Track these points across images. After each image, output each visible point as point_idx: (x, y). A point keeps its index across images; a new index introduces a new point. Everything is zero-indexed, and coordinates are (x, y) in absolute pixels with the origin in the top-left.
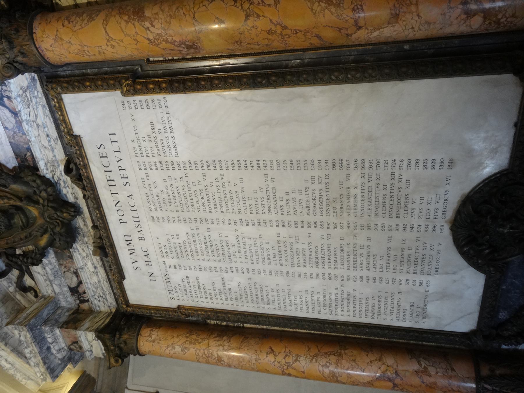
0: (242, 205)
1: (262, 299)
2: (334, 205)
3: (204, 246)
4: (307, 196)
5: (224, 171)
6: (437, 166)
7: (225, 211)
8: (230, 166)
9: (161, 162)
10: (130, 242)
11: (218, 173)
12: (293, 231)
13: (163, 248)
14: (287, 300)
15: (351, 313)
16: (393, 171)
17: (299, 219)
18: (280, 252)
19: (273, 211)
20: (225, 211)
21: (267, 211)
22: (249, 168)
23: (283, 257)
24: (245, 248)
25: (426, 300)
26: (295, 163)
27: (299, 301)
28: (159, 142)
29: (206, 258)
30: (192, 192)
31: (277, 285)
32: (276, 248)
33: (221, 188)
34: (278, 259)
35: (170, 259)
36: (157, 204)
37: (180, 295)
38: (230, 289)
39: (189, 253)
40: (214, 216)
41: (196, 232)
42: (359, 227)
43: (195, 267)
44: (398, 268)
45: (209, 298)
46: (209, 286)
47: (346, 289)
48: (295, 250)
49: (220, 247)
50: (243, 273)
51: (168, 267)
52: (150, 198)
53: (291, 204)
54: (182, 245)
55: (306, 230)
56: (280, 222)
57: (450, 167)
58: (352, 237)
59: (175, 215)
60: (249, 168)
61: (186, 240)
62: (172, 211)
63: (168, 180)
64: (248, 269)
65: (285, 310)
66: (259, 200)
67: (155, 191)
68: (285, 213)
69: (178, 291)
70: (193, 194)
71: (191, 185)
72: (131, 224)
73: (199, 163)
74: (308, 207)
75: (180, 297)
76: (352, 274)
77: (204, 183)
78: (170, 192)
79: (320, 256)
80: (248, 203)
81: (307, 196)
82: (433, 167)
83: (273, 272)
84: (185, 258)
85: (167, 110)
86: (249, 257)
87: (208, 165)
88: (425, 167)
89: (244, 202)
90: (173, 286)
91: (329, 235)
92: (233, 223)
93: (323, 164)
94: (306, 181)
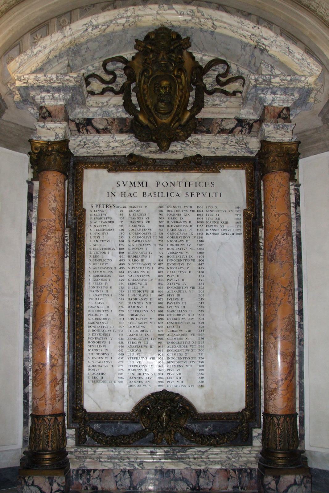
0: (173, 270)
1: (98, 276)
2: (175, 327)
3: (141, 239)
4: (181, 311)
5: (196, 262)
6: (199, 380)
7: (169, 258)
8: (200, 266)
9: (202, 222)
10: (142, 185)
11: (195, 256)
12: (156, 301)
13: (138, 209)
14: (99, 293)
15: (91, 336)
16: (197, 358)
17: (165, 305)
18: (139, 291)
19: (169, 290)
20: (169, 258)
21: (170, 286)
22: (199, 278)
23: (135, 294)
24: (141, 268)
25: (108, 382)
26: (202, 305)
27: (98, 301)
28: (216, 224)
29: (131, 240)
30: (182, 239)
31: (111, 287)
32: (142, 289)
33: (185, 258)
34: (134, 290)
35: (129, 213)
36: (173, 213)
37: (96, 213)
38: (105, 253)
39: (134, 228)
40: (165, 250)
41: (152, 235)
42: (160, 341)
43: (123, 230)
44: (132, 364)
45: (95, 236)
46: (106, 237)
47: (112, 333)
48: (141, 301)
49: (141, 251)
50: (120, 264)
51: (122, 209)
52: (177, 209)
53: (175, 301)
54: (141, 224)
55: (157, 310)
56: (162, 293)
57: (199, 386)
58: (153, 337)
59: (165, 224)
60: (199, 278)
61: (145, 228)
62: (168, 222)
63: (190, 224)
64: (123, 268)
65: (89, 291)
66: (177, 282)
67: (183, 214)
68: (168, 297)
69: (100, 213)
70: (180, 239)
71: (187, 239)
72: (157, 190)
73: (202, 247)
74: (173, 311)
75: (93, 213)
76: (125, 337)
77: (189, 247)
78: (182, 224)
79: (138, 317)
80: (175, 275)
81: (181, 311)
82: (199, 378)
83: (122, 286)
84: (130, 224)
85: (235, 234)
86: (134, 270)
87: (201, 253)
88: (199, 374)
89: (176, 272)
90: (104, 209)
91: (154, 323)
92: (160, 262)
93: (201, 321)
94: (191, 311)
